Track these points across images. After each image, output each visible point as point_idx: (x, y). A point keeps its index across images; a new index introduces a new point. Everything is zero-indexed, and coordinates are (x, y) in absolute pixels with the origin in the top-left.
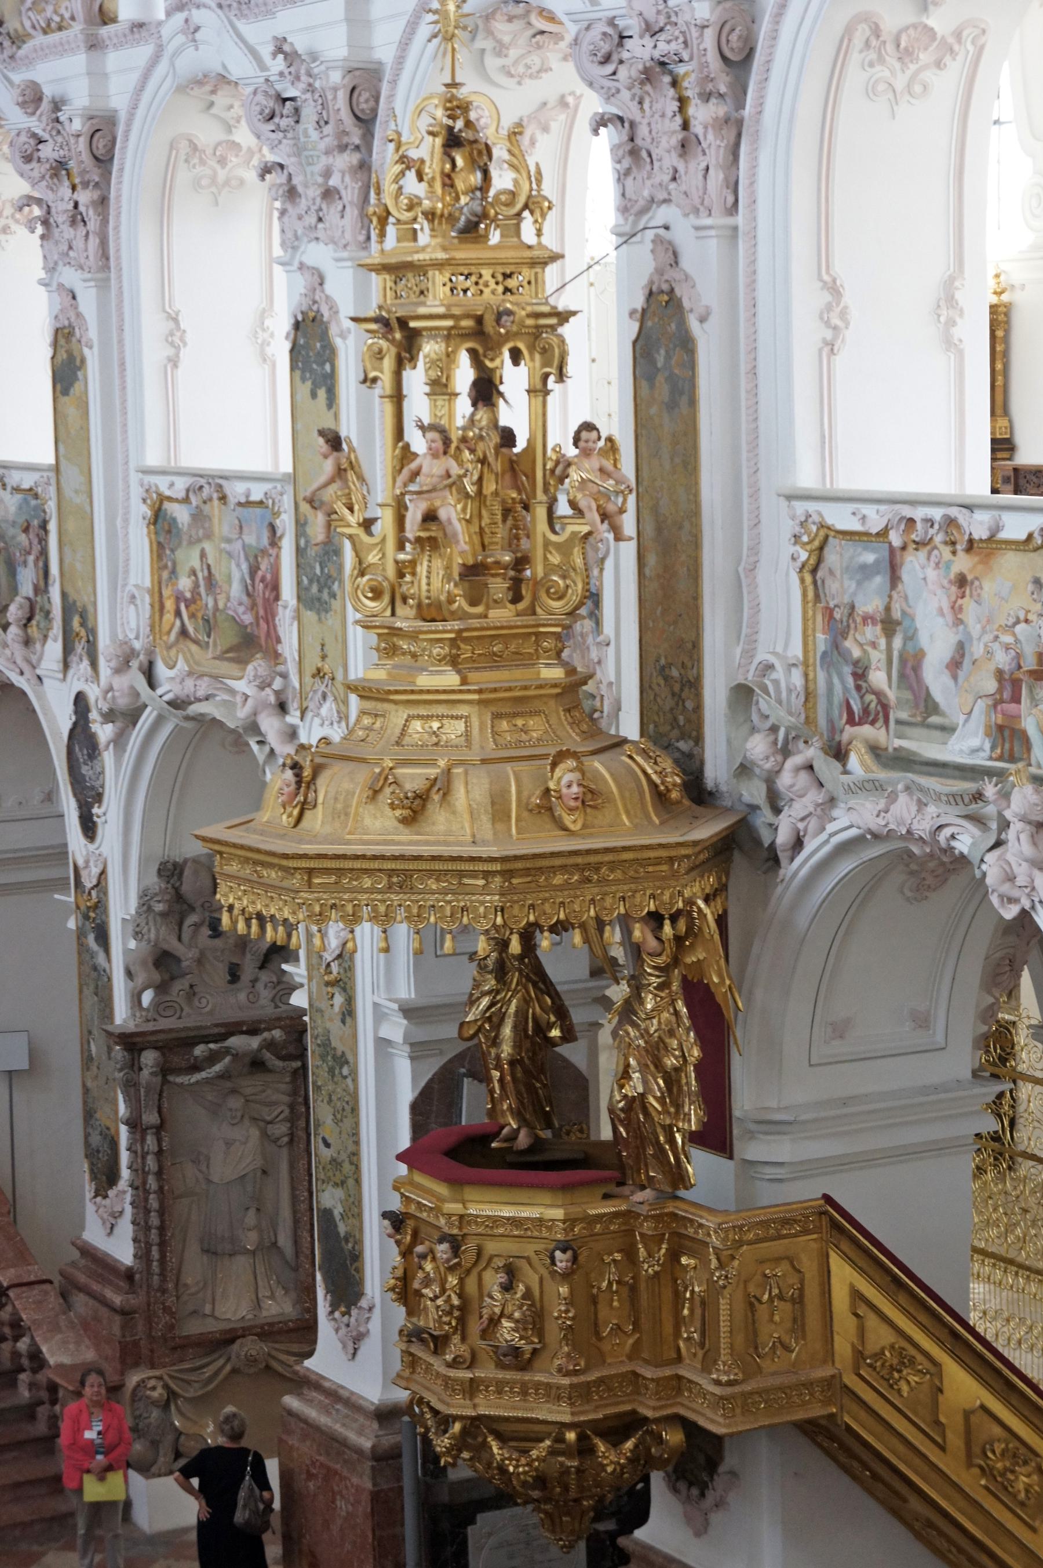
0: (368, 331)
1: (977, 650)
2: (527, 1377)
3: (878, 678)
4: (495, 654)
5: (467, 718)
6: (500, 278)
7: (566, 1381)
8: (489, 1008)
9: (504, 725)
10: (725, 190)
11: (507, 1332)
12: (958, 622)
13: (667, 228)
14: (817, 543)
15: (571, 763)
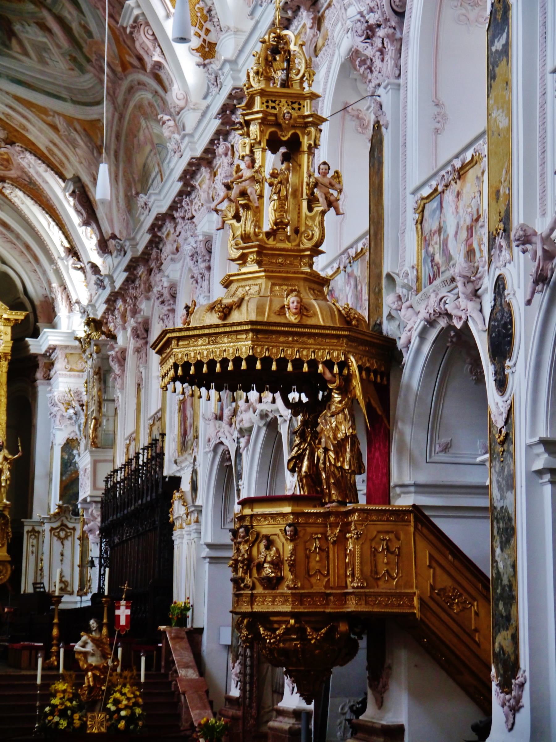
0: (241, 135)
1: (462, 223)
2: (274, 591)
3: (437, 258)
4: (279, 263)
5: (261, 285)
6: (290, 103)
7: (290, 591)
8: (297, 451)
9: (277, 288)
10: (395, 69)
11: (268, 570)
12: (457, 212)
13: (379, 96)
14: (421, 209)
15: (295, 293)
